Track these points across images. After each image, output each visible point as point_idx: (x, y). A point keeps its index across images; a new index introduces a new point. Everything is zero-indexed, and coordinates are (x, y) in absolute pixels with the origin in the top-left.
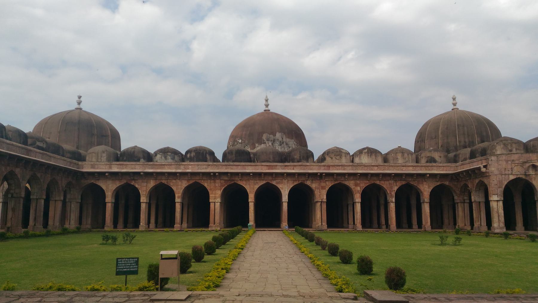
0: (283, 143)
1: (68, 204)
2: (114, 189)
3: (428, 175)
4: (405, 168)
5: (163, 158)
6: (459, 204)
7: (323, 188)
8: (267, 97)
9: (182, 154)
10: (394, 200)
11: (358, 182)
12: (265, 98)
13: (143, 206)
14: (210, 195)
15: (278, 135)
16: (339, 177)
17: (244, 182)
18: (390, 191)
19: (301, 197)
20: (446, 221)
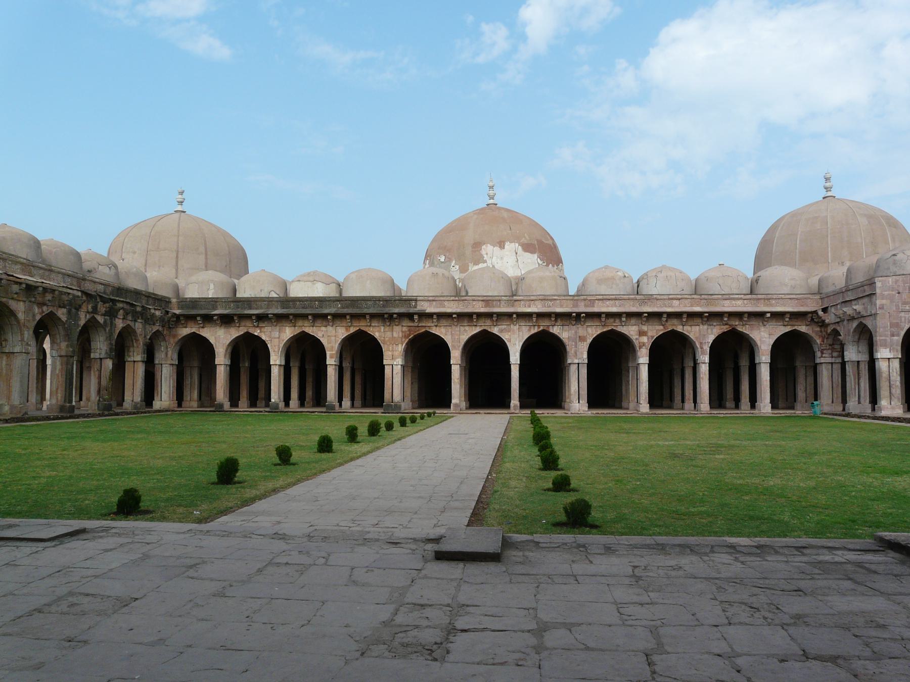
3: (768, 315)
4: (728, 302)
7: (582, 339)
11: (645, 328)
13: (276, 374)
14: (387, 354)
16: (611, 320)
18: (701, 343)
19: (545, 354)
20: (801, 395)
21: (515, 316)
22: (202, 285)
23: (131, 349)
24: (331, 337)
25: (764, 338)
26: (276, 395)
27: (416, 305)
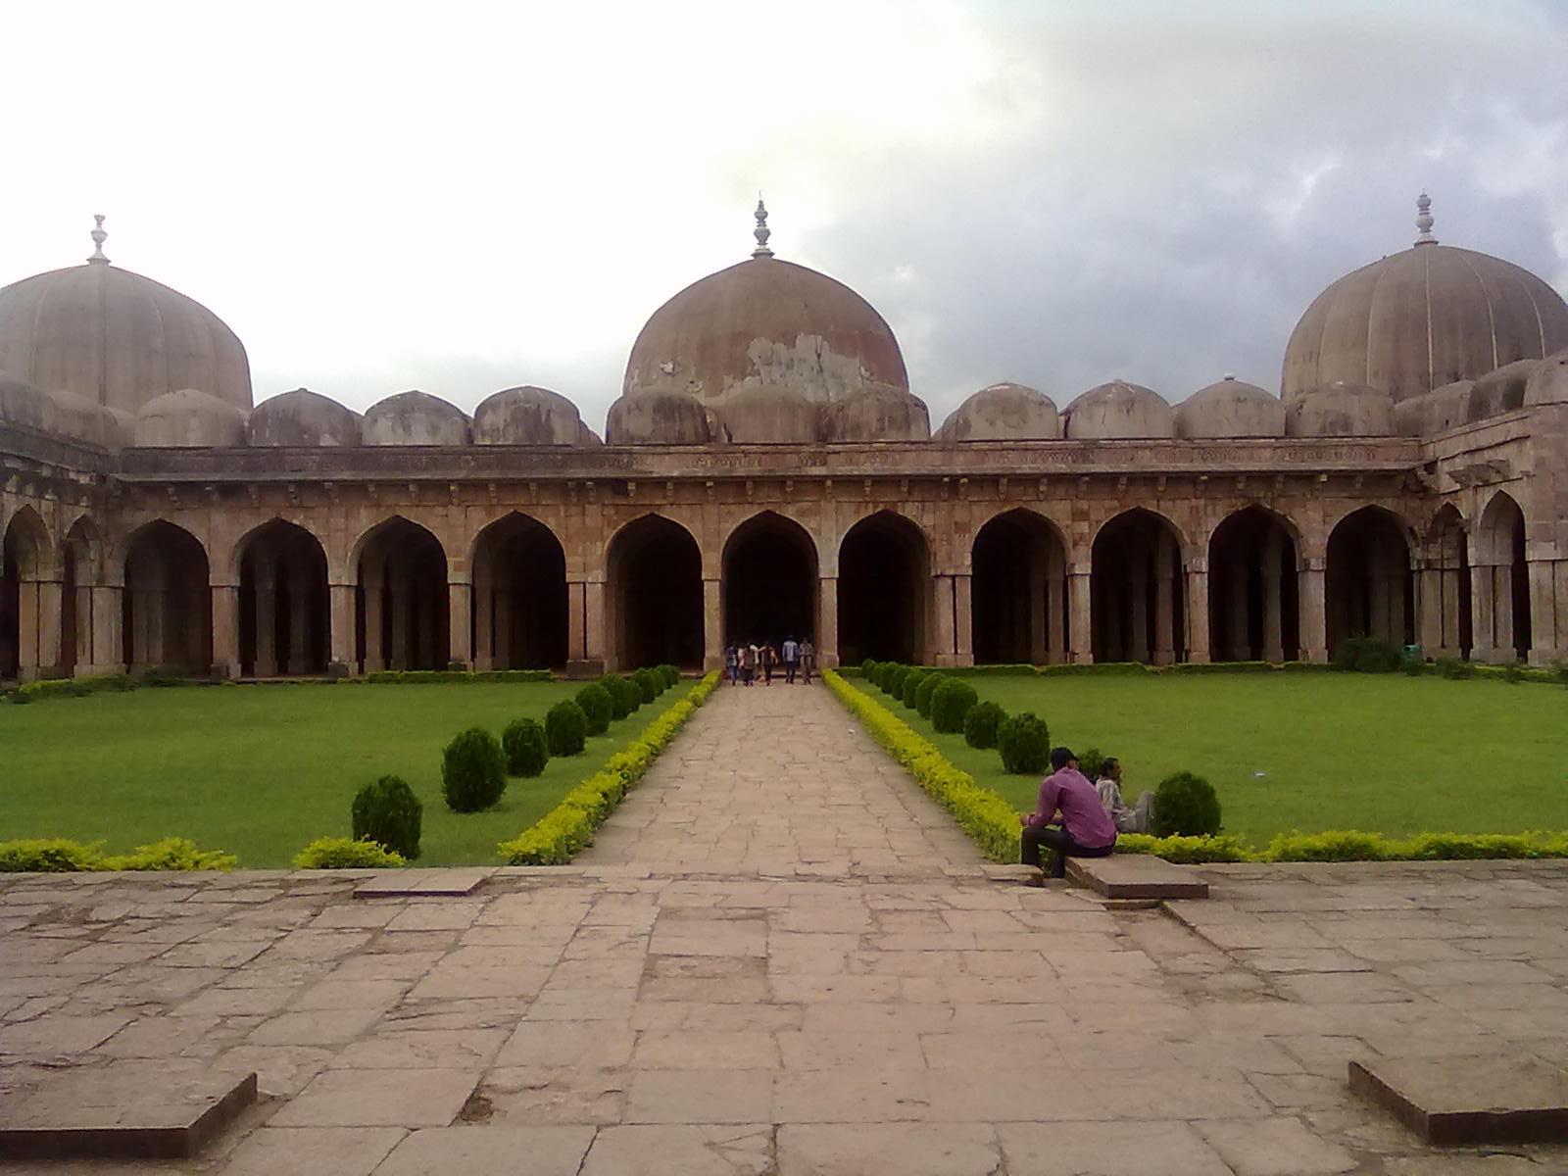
1: (82, 596)
2: (236, 540)
3: (1324, 478)
5: (400, 430)
6: (1426, 576)
7: (961, 528)
8: (761, 202)
9: (464, 416)
10: (1205, 568)
11: (1084, 505)
12: (755, 208)
13: (341, 604)
14: (569, 560)
15: (806, 344)
17: (685, 512)
18: (1193, 535)
19: (886, 560)
21: (829, 483)
23: (31, 556)
24: (458, 532)
25: (1315, 526)
26: (341, 649)
27: (629, 465)
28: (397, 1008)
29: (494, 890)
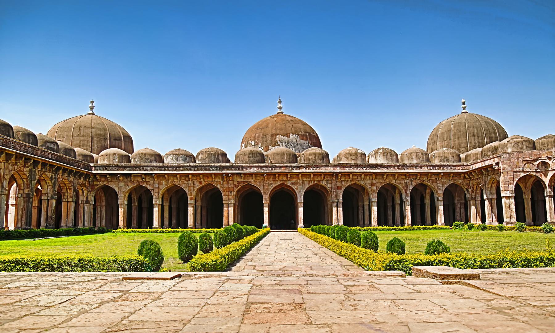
0: (297, 145)
1: (81, 206)
5: (174, 159)
7: (339, 188)
15: (292, 137)
16: (356, 177)
22: (107, 156)
28: (117, 325)
29: (182, 279)
